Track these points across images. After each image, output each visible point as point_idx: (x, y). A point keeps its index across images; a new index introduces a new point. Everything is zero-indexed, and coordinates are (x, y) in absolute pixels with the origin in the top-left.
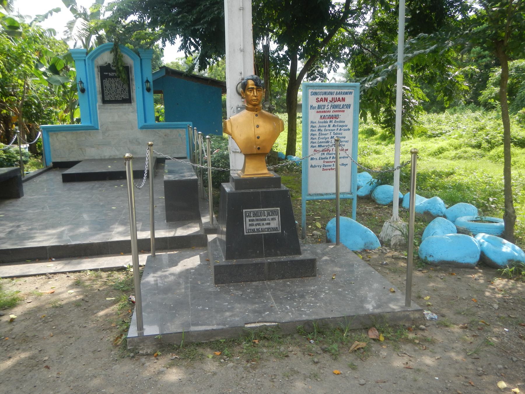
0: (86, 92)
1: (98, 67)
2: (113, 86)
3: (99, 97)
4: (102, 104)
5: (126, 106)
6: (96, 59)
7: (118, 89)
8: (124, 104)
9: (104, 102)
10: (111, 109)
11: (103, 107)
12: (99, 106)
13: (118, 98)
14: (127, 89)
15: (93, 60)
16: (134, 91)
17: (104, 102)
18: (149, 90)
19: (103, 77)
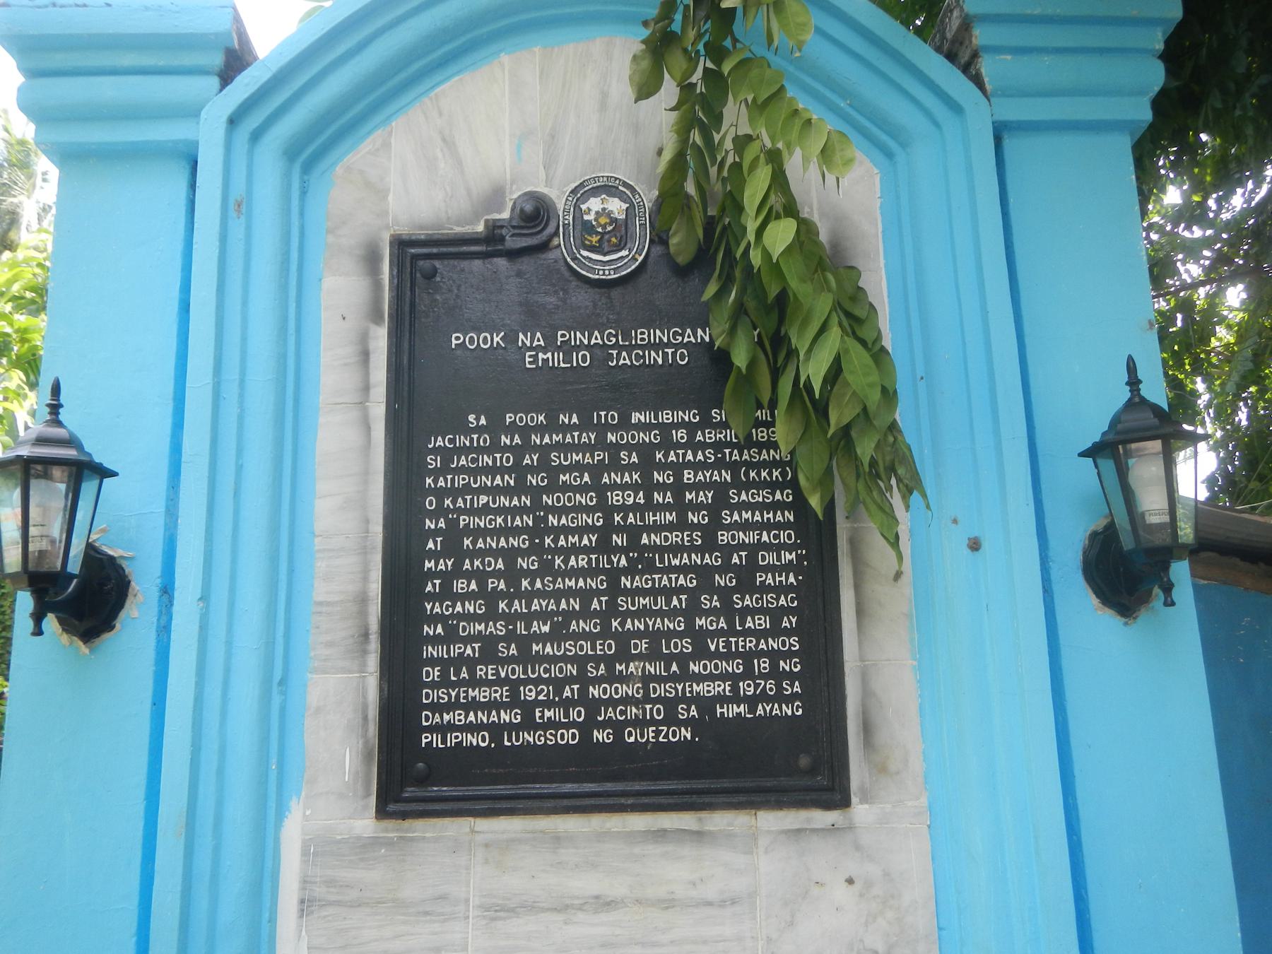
0: (137, 616)
1: (371, 259)
2: (573, 514)
3: (337, 703)
4: (366, 824)
5: (747, 855)
6: (358, 157)
7: (643, 562)
8: (719, 820)
9: (415, 774)
10: (498, 910)
11: (372, 876)
12: (315, 849)
13: (638, 704)
14: (782, 560)
15: (312, 152)
16: (893, 601)
17: (415, 774)
18: (1123, 571)
19: (419, 408)
